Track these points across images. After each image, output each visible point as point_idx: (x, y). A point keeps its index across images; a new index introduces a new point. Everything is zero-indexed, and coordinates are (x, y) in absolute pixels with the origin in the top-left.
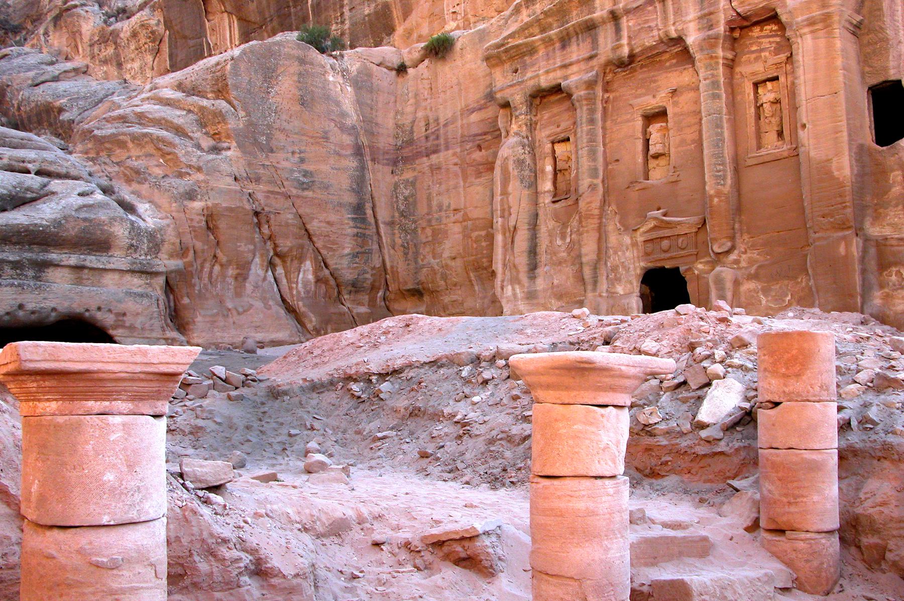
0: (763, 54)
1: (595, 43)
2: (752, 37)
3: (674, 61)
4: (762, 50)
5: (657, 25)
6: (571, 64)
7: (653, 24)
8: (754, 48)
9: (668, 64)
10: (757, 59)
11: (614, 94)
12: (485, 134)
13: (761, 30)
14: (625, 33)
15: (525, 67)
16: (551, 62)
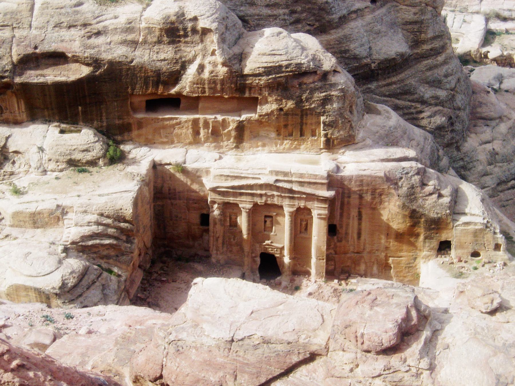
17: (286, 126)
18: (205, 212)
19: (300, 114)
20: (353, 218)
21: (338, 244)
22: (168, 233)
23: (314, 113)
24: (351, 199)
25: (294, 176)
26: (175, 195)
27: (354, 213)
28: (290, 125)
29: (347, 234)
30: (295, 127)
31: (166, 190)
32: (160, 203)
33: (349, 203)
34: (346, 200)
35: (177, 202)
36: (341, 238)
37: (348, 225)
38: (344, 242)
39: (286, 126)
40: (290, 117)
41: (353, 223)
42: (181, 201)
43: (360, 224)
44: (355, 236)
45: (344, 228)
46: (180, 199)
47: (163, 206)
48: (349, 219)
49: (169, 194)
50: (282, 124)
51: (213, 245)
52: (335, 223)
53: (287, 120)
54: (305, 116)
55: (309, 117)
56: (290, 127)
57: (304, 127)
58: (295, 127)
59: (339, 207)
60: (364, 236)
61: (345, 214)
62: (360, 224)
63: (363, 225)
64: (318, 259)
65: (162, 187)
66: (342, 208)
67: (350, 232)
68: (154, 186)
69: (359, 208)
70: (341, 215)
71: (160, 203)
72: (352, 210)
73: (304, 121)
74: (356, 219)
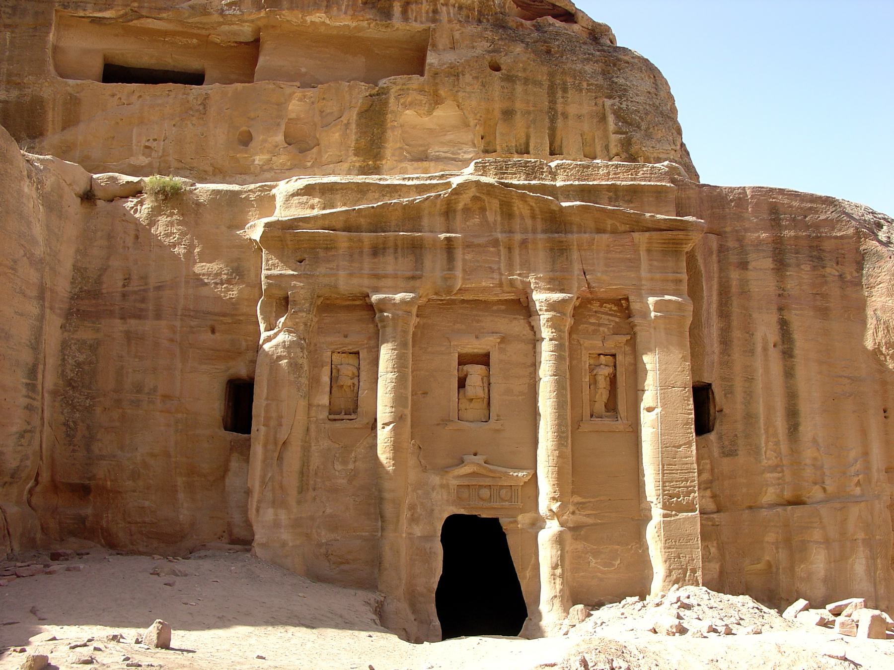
0: (601, 329)
1: (419, 262)
2: (590, 310)
3: (503, 307)
4: (600, 325)
5: (499, 269)
6: (385, 276)
7: (495, 267)
8: (593, 320)
9: (495, 308)
10: (595, 332)
11: (425, 321)
12: (224, 315)
13: (601, 306)
14: (459, 264)
15: (316, 260)
16: (356, 265)
17: (508, 114)
18: (241, 370)
19: (546, 84)
20: (765, 349)
21: (726, 464)
22: (102, 457)
23: (585, 85)
24: (751, 275)
25: (559, 178)
26: (143, 300)
27: (766, 329)
28: (519, 113)
29: (750, 418)
30: (534, 121)
31: (113, 283)
32: (86, 334)
33: (744, 293)
34: (735, 275)
35: (147, 326)
36: (733, 443)
37: (750, 379)
38: (742, 458)
39: (508, 114)
40: (519, 88)
41: (767, 370)
42: (163, 323)
43: (789, 373)
44: (780, 423)
45: (739, 396)
46: (158, 316)
47: (94, 347)
48: (752, 352)
49: (124, 295)
50: (498, 107)
51: (263, 483)
52: (707, 381)
53: (511, 98)
54: (560, 94)
55: (570, 93)
56: (519, 121)
57: (560, 123)
58: (534, 121)
59: (714, 306)
60: (812, 425)
61: (737, 334)
62: (789, 373)
63: (801, 372)
64: (671, 506)
65: (104, 270)
66: (724, 314)
67: (761, 409)
68: (76, 268)
69: (780, 309)
70: (725, 342)
71: (86, 334)
72: (755, 315)
73: (559, 107)
74: (775, 355)
